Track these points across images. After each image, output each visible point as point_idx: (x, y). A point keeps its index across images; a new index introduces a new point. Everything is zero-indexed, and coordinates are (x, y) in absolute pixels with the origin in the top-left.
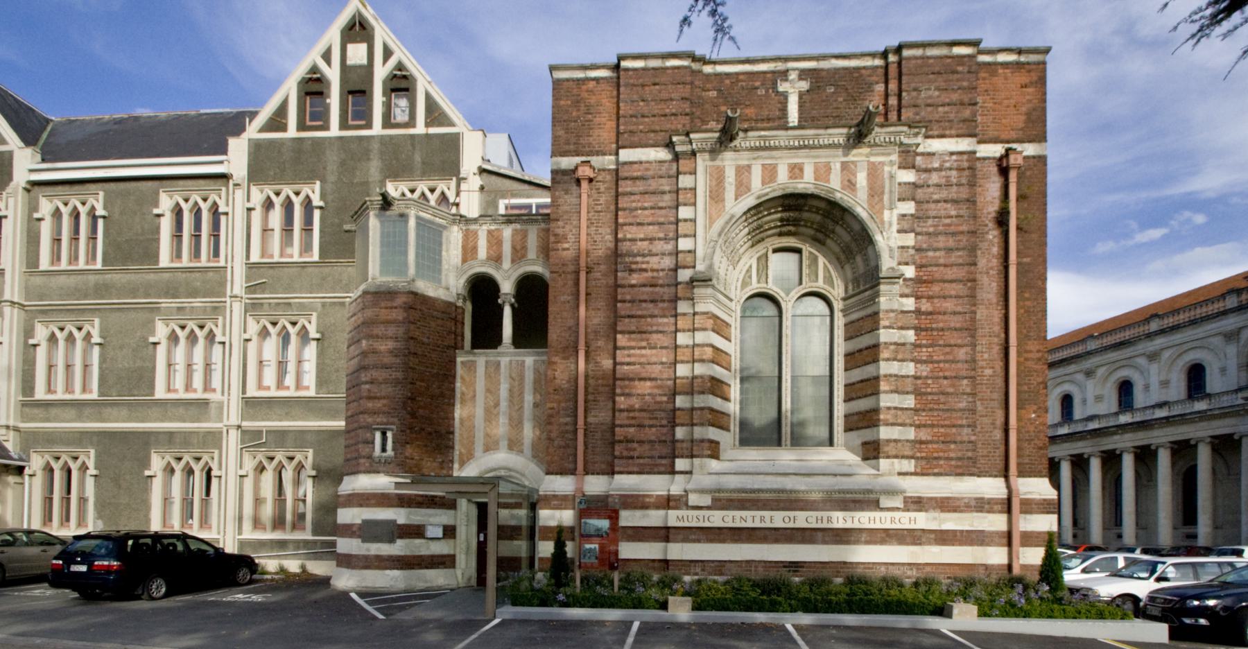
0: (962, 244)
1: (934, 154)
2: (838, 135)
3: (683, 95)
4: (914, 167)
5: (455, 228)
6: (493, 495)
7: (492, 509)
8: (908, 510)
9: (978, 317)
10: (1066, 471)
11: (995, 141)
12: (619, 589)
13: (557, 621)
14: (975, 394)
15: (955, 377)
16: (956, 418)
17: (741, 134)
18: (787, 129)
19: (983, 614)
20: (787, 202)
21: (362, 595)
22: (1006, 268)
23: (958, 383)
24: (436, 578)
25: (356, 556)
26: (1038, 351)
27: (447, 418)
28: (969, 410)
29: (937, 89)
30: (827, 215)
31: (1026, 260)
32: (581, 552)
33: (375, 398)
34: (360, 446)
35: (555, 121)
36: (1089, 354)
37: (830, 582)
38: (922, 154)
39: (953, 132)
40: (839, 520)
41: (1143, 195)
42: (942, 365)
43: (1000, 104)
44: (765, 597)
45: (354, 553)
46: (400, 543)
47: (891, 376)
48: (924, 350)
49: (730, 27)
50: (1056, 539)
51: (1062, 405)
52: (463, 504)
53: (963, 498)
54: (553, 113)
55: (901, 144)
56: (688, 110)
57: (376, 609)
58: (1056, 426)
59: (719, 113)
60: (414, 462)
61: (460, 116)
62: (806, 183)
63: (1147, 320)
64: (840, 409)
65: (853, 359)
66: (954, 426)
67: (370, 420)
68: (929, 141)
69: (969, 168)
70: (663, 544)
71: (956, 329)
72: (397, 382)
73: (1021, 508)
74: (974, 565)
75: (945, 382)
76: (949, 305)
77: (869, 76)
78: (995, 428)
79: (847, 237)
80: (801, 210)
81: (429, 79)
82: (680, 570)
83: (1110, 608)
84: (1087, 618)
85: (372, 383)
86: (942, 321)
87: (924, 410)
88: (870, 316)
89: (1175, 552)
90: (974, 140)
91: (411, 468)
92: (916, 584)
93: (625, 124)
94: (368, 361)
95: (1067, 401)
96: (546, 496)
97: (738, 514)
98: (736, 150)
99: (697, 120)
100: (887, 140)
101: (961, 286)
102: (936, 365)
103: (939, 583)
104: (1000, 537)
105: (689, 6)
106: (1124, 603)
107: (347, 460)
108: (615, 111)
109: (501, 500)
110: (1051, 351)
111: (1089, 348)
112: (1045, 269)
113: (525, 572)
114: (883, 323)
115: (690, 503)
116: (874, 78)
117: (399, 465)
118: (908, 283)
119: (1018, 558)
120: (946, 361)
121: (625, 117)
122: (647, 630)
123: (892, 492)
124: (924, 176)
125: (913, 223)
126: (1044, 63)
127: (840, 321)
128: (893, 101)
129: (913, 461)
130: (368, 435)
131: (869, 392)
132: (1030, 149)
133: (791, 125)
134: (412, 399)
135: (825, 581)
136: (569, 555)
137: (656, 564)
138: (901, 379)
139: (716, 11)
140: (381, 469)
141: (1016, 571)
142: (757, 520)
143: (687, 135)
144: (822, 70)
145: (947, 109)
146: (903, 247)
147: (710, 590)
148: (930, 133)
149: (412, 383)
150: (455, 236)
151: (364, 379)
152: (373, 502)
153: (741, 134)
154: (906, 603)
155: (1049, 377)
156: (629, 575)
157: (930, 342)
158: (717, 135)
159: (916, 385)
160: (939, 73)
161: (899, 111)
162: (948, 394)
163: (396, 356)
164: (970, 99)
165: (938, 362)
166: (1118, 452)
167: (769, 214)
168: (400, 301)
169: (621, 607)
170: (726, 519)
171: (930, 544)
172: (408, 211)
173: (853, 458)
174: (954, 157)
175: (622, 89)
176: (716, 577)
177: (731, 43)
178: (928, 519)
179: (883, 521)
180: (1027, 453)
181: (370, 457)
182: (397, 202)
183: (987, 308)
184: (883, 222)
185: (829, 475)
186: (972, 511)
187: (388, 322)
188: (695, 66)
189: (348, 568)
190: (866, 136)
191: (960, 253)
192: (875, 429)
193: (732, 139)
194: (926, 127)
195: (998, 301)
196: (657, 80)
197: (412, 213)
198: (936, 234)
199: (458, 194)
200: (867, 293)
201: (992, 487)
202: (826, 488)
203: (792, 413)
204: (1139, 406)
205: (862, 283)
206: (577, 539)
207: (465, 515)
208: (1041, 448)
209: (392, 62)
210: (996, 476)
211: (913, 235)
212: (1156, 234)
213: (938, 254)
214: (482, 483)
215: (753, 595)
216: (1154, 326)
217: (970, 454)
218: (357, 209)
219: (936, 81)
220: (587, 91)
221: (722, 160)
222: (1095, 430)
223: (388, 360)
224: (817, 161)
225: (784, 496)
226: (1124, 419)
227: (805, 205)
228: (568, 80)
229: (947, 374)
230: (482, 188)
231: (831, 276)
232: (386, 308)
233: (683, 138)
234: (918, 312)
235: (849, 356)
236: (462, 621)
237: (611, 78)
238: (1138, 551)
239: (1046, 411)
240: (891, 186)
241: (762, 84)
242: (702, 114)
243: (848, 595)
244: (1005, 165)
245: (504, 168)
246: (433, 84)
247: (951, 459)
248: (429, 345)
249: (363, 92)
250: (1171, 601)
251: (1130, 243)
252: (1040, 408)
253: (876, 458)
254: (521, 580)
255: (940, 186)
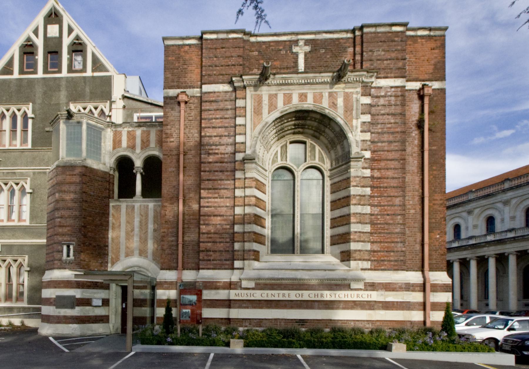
0: (397, 139)
1: (381, 88)
2: (327, 77)
3: (239, 54)
4: (370, 95)
5: (109, 130)
6: (130, 281)
7: (130, 289)
8: (367, 290)
9: (407, 180)
10: (456, 268)
11: (416, 80)
12: (202, 335)
13: (167, 353)
14: (405, 224)
15: (394, 215)
16: (394, 238)
17: (272, 76)
18: (298, 73)
19: (409, 349)
20: (298, 115)
21: (56, 338)
22: (423, 152)
23: (395, 218)
24: (98, 328)
25: (53, 316)
26: (441, 200)
27: (104, 238)
28: (401, 233)
29: (383, 50)
30: (320, 122)
31: (434, 148)
32: (180, 314)
33: (63, 226)
34: (55, 254)
35: (166, 69)
36: (470, 201)
37: (322, 331)
38: (375, 88)
39: (392, 75)
40: (328, 295)
41: (501, 111)
42: (386, 208)
43: (419, 59)
44: (285, 340)
45: (51, 314)
46: (77, 309)
47: (357, 214)
48: (376, 199)
49: (265, 15)
50: (451, 307)
51: (455, 230)
52: (113, 286)
53: (398, 283)
54: (165, 64)
55: (363, 82)
56: (241, 63)
57: (64, 346)
58: (451, 242)
59: (259, 64)
60: (86, 263)
61: (112, 66)
62: (309, 104)
63: (503, 182)
64: (328, 233)
65: (335, 204)
66: (393, 242)
67: (60, 239)
68: (379, 80)
69: (401, 96)
70: (227, 309)
71: (394, 187)
72: (76, 217)
73: (431, 289)
74: (404, 321)
75: (388, 217)
76: (390, 173)
77: (345, 43)
78: (416, 243)
79: (332, 135)
80: (306, 119)
81: (94, 45)
82: (237, 324)
83: (482, 345)
84: (469, 351)
85: (61, 218)
86: (386, 183)
87: (376, 233)
88: (345, 179)
89: (519, 314)
90: (404, 79)
91: (84, 266)
92: (371, 332)
93: (206, 71)
94: (58, 206)
95: (457, 228)
96: (160, 282)
97: (270, 292)
98: (269, 85)
99: (246, 68)
100: (355, 79)
101: (397, 163)
102: (383, 208)
103: (384, 332)
104: (419, 305)
105: (242, 3)
106: (490, 343)
107: (47, 262)
108: (200, 63)
109: (135, 284)
110: (448, 200)
111: (470, 198)
112: (445, 153)
113: (148, 325)
114: (352, 184)
115: (243, 286)
116: (347, 45)
117: (77, 264)
118: (367, 161)
119: (429, 317)
120: (388, 206)
121: (205, 66)
122: (218, 358)
123: (357, 280)
124: (376, 100)
125: (370, 126)
126: (444, 36)
127: (328, 183)
128: (358, 58)
129: (369, 262)
130: (60, 247)
131: (345, 223)
132: (436, 85)
133: (300, 71)
134: (85, 227)
135: (319, 331)
136: (174, 316)
137: (223, 321)
138: (362, 216)
139: (257, 6)
140: (67, 267)
141: (428, 324)
142: (281, 296)
143: (241, 76)
144: (318, 40)
145: (389, 62)
146: (364, 141)
147: (254, 335)
148: (379, 76)
149: (84, 218)
150: (108, 134)
151: (57, 216)
152: (62, 285)
153: (272, 76)
154: (366, 343)
155: (447, 215)
156: (208, 327)
157: (379, 194)
158: (258, 77)
159: (371, 219)
160: (384, 42)
161: (362, 63)
162: (389, 224)
163: (75, 202)
164: (402, 57)
165: (384, 206)
166: (486, 257)
167: (288, 122)
168: (77, 171)
169: (203, 345)
170: (263, 295)
171: (379, 309)
172: (82, 120)
173: (335, 261)
174: (393, 89)
175: (204, 51)
176: (257, 328)
177: (266, 24)
178: (378, 295)
179: (352, 296)
180: (435, 257)
181: (60, 260)
182: (76, 115)
183: (412, 175)
184: (352, 126)
185: (321, 270)
186: (403, 291)
187: (71, 183)
188: (246, 38)
189: (48, 323)
190: (343, 77)
191: (396, 144)
192: (348, 244)
193: (266, 79)
194: (377, 72)
195: (418, 171)
196: (224, 46)
197: (84, 121)
198: (383, 133)
199: (110, 111)
200: (343, 167)
201: (415, 277)
202: (320, 278)
203: (301, 234)
204: (498, 231)
205: (340, 161)
206: (178, 306)
207: (115, 291)
208: (442, 255)
209: (73, 35)
210: (417, 271)
211: (369, 134)
212: (507, 133)
213: (384, 144)
214: (124, 275)
215: (279, 338)
216: (507, 185)
217: (402, 258)
218: (53, 119)
219: (382, 46)
220: (184, 52)
221: (261, 91)
222: (473, 245)
223: (70, 205)
224: (315, 91)
225: (296, 282)
226: (490, 238)
227: (308, 116)
228: (173, 45)
229: (389, 212)
230: (124, 107)
231: (323, 157)
232: (70, 175)
233: (238, 78)
234: (372, 177)
235: (333, 202)
236: (113, 353)
237: (198, 44)
238: (498, 313)
239: (445, 234)
240: (357, 106)
241: (284, 48)
242: (250, 65)
243: (332, 338)
244: (422, 94)
245: (137, 96)
246: (96, 48)
247: (391, 261)
248: (94, 196)
249: (56, 52)
250: (516, 342)
251: (493, 138)
252: (442, 232)
253: (349, 260)
254: (146, 330)
255: (385, 106)
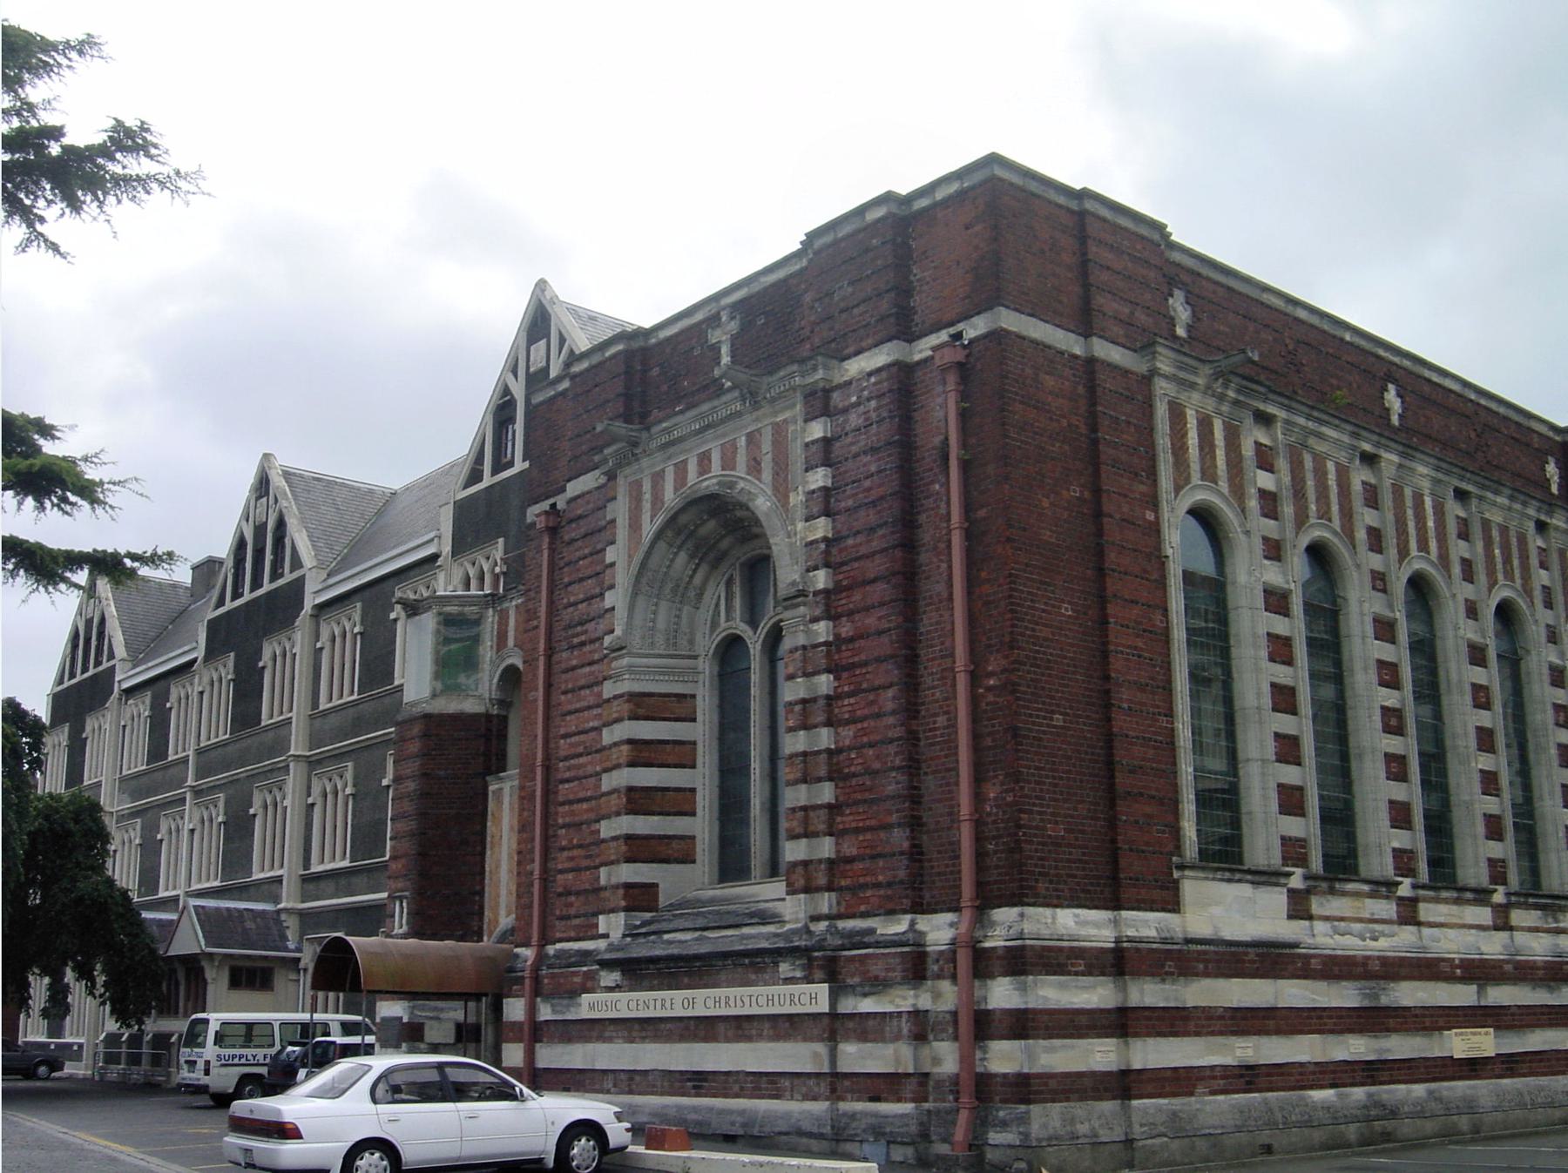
39: (870, 341)
76: (871, 621)
102: (859, 726)
165: (865, 718)
174: (873, 380)
